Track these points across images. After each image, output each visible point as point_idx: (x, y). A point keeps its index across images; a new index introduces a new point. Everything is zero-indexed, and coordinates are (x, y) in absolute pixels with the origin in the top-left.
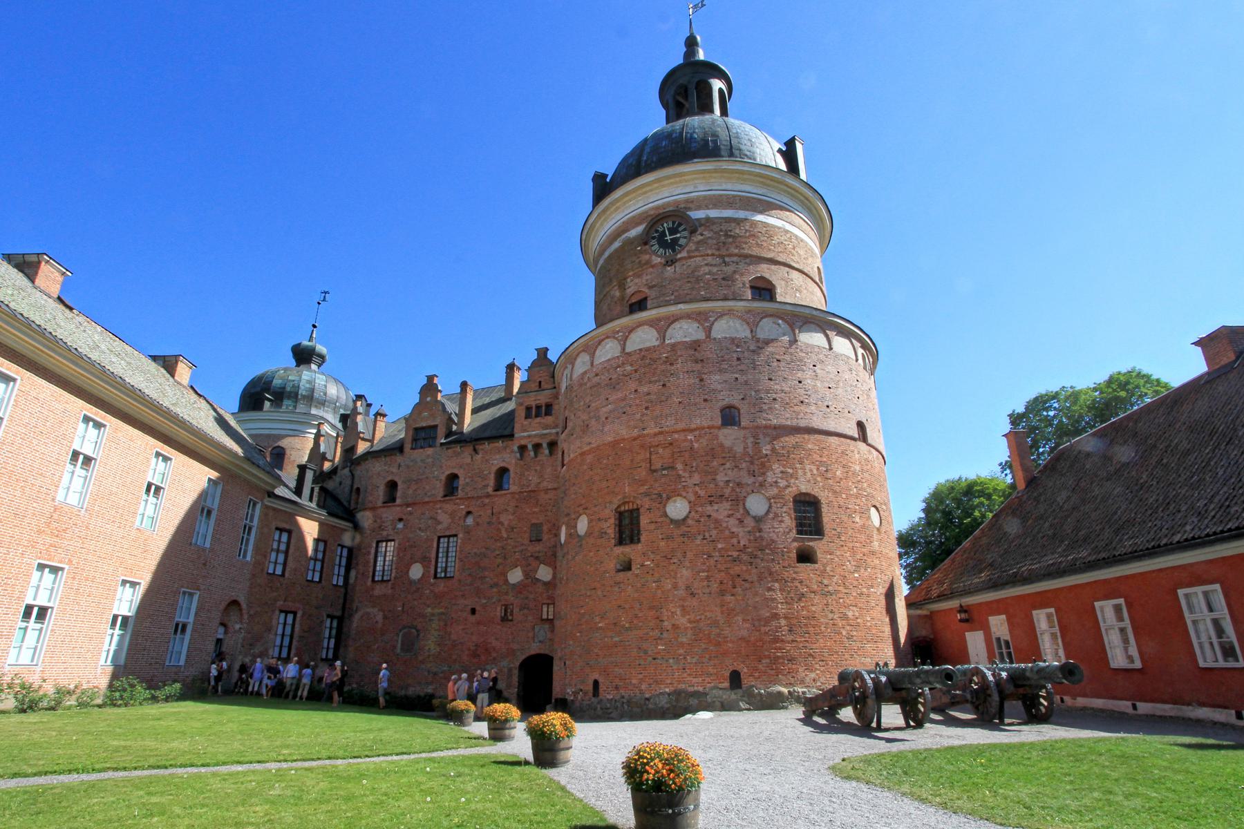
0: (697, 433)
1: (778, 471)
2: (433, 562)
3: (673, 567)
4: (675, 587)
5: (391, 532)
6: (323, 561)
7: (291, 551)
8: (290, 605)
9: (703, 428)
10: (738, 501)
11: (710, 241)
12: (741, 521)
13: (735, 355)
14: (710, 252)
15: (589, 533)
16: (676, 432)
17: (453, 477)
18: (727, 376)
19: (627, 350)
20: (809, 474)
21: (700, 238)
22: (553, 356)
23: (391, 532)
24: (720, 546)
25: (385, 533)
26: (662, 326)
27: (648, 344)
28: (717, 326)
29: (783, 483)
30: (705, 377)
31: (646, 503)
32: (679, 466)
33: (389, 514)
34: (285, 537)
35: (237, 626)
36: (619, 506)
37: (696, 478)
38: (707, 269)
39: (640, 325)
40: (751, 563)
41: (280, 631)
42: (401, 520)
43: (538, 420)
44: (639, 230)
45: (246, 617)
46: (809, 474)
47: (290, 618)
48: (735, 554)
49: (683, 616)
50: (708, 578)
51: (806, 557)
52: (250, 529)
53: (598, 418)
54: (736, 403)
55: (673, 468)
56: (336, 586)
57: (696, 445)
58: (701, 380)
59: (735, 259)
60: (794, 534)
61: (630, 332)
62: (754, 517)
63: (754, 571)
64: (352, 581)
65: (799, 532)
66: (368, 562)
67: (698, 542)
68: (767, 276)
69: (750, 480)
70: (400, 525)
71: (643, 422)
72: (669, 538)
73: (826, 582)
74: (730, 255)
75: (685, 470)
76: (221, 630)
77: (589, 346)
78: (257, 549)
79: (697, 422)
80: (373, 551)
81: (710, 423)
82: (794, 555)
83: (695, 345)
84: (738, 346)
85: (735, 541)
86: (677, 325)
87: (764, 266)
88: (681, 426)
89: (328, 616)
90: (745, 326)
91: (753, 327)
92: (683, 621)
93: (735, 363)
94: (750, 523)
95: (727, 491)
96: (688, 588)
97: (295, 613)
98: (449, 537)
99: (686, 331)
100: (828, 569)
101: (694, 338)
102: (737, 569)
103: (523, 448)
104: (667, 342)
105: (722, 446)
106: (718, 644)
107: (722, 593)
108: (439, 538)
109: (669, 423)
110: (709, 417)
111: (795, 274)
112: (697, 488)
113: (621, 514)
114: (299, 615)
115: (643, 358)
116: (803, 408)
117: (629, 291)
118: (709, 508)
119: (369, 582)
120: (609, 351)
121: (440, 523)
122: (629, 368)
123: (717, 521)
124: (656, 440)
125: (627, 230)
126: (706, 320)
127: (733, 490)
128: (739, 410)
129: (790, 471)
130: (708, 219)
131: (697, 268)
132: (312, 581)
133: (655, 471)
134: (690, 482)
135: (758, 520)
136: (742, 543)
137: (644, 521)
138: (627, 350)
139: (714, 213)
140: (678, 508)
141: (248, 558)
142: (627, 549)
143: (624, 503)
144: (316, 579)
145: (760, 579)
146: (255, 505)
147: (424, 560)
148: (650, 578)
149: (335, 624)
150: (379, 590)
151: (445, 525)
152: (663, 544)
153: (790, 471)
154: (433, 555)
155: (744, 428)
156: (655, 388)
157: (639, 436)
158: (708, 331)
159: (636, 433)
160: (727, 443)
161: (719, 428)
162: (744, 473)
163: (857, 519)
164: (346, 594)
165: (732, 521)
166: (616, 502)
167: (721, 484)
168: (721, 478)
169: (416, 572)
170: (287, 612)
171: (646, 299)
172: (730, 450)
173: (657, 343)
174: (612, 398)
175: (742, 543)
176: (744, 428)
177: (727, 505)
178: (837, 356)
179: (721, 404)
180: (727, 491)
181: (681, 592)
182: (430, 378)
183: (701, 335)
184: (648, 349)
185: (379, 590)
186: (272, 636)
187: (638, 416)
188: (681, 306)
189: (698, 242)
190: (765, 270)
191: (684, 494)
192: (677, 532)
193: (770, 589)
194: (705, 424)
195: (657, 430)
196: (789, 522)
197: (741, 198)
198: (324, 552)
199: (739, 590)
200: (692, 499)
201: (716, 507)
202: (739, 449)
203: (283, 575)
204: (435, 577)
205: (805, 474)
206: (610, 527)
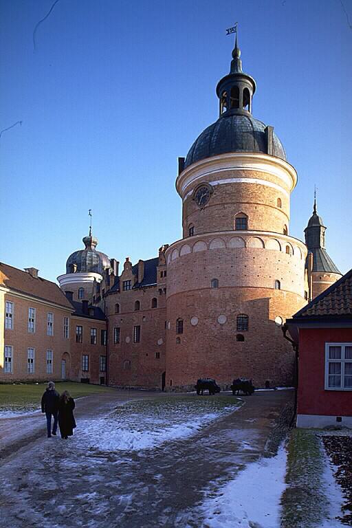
10: (215, 318)
12: (215, 326)
17: (138, 302)
26: (192, 244)
27: (187, 253)
28: (211, 245)
31: (184, 318)
32: (196, 305)
33: (117, 318)
44: (190, 193)
47: (87, 357)
51: (241, 338)
55: (193, 305)
59: (229, 205)
74: (227, 204)
83: (204, 253)
88: (197, 288)
95: (211, 314)
99: (200, 247)
103: (160, 290)
107: (207, 352)
113: (179, 322)
115: (186, 259)
117: (189, 223)
120: (186, 250)
121: (134, 321)
124: (189, 294)
125: (188, 192)
130: (218, 185)
131: (212, 212)
135: (222, 325)
139: (221, 182)
140: (194, 321)
149: (104, 358)
151: (137, 321)
158: (208, 246)
162: (218, 307)
168: (209, 309)
174: (177, 276)
178: (267, 251)
180: (211, 314)
193: (224, 351)
196: (234, 325)
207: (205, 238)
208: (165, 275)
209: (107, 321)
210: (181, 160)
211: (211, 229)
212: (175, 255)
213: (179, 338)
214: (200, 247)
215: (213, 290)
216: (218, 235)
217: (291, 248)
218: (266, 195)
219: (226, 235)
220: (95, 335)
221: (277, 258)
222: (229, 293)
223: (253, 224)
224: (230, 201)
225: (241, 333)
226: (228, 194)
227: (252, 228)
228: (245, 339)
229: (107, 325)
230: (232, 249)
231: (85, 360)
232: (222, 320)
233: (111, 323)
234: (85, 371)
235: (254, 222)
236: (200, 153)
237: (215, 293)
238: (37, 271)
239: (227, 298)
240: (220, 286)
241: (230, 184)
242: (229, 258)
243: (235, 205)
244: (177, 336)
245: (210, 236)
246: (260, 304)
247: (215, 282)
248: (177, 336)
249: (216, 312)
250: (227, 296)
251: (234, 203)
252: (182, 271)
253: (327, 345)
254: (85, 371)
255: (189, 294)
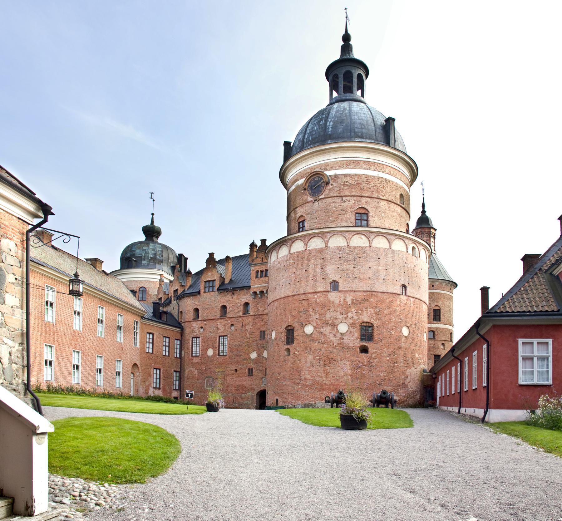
0: (319, 294)
1: (354, 312)
2: (217, 348)
3: (306, 355)
4: (306, 362)
5: (198, 333)
6: (169, 346)
7: (155, 342)
8: (157, 366)
9: (322, 292)
10: (334, 326)
11: (336, 189)
12: (335, 335)
13: (339, 256)
14: (335, 195)
15: (276, 338)
16: (310, 293)
18: (334, 267)
19: (292, 252)
20: (369, 313)
21: (331, 186)
22: (268, 244)
23: (198, 333)
24: (325, 346)
25: (195, 334)
29: (355, 318)
30: (323, 267)
32: (311, 310)
34: (151, 336)
35: (138, 374)
36: (286, 327)
37: (317, 316)
38: (333, 205)
39: (297, 239)
40: (338, 353)
41: (155, 377)
42: (202, 327)
43: (262, 279)
45: (140, 370)
46: (369, 313)
47: (158, 371)
48: (331, 349)
49: (309, 374)
50: (319, 359)
51: (364, 350)
52: (137, 333)
53: (279, 285)
54: (337, 279)
55: (308, 311)
56: (176, 357)
57: (318, 300)
58: (322, 268)
59: (348, 198)
60: (359, 340)
61: (293, 243)
62: (341, 333)
63: (339, 356)
64: (183, 355)
65: (361, 339)
66: (189, 347)
67: (316, 344)
68: (365, 206)
69: (340, 317)
70: (202, 330)
71: (296, 289)
72: (305, 342)
73: (371, 361)
75: (313, 312)
76: (132, 375)
77: (280, 243)
78: (140, 342)
79: (319, 289)
80: (191, 342)
81: (325, 290)
82: (358, 350)
83: (321, 251)
84: (340, 251)
85: (332, 344)
86: (313, 240)
87: (364, 200)
89: (174, 371)
90: (345, 240)
91: (348, 240)
92: (308, 377)
93: (338, 260)
94: (339, 336)
95: (330, 322)
96: (311, 363)
97: (160, 369)
98: (224, 336)
100: (373, 356)
101: (320, 247)
102: (331, 356)
103: (255, 293)
104: (308, 249)
105: (329, 300)
106: (322, 386)
108: (220, 336)
109: (307, 290)
110: (324, 286)
111: (383, 203)
112: (317, 320)
113: (288, 330)
114: (162, 370)
115: (298, 257)
116: (370, 281)
118: (322, 329)
119: (190, 357)
122: (292, 261)
123: (325, 335)
126: (326, 237)
127: (333, 321)
128: (338, 283)
129: (360, 312)
130: (336, 176)
132: (165, 356)
133: (301, 312)
134: (315, 317)
135: (343, 334)
136: (335, 345)
137: (296, 334)
138: (292, 252)
140: (309, 329)
141: (138, 346)
142: (289, 347)
143: (289, 326)
144: (167, 354)
145: (341, 360)
146: (137, 322)
147: (214, 348)
148: (296, 359)
149: (178, 374)
150: (195, 360)
152: (302, 344)
153: (360, 312)
154: (217, 345)
155: (341, 291)
156: (302, 272)
157: (295, 295)
158: (326, 243)
159: (294, 293)
160: (332, 299)
161: (328, 291)
162: (338, 313)
163: (393, 333)
164: (181, 361)
165: (331, 336)
166: (286, 325)
167: (328, 318)
168: (328, 316)
169: (210, 352)
170: (156, 369)
171: (305, 220)
172: (333, 303)
173: (304, 249)
175: (335, 345)
176: (341, 291)
177: (329, 328)
178: (393, 252)
179: (330, 280)
180: (330, 322)
181: (308, 365)
182: (211, 255)
183: (323, 246)
184: (300, 252)
185: (195, 360)
186: (152, 379)
187: (294, 286)
188: (314, 231)
189: (330, 189)
190: (364, 202)
191: (312, 323)
192: (308, 340)
193: (345, 364)
194: (322, 290)
195: (302, 292)
196: (357, 335)
197: (354, 161)
198: (169, 342)
199: (332, 365)
200: (315, 324)
201: (325, 329)
202: (337, 302)
203: (153, 353)
204: (219, 355)
205: (367, 313)
206: (283, 336)
207: (323, 233)
208: (266, 276)
209: (182, 329)
210: (287, 144)
211: (328, 224)
212: (284, 251)
213: (288, 350)
214: (316, 244)
215: (331, 294)
216: (337, 232)
217: (417, 249)
218: (388, 189)
219: (347, 231)
220: (167, 344)
221: (404, 259)
222: (351, 297)
223: (373, 221)
224: (349, 194)
225: (364, 344)
226: (347, 185)
227: (375, 225)
228: (370, 350)
229: (182, 334)
230: (355, 248)
231: (155, 374)
232: (343, 328)
233: (187, 331)
234: (156, 388)
235: (376, 219)
236: (312, 139)
237: (334, 297)
238: (102, 262)
239: (348, 303)
240: (340, 288)
241: (349, 175)
242: (351, 257)
243: (355, 198)
244: (286, 347)
245: (329, 232)
246: (385, 312)
247: (335, 285)
248: (286, 347)
249: (336, 319)
250: (349, 300)
251: (354, 196)
252: (293, 270)
253: (520, 341)
254: (156, 388)
255: (303, 297)
